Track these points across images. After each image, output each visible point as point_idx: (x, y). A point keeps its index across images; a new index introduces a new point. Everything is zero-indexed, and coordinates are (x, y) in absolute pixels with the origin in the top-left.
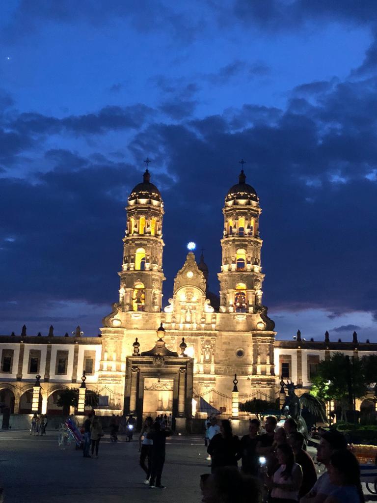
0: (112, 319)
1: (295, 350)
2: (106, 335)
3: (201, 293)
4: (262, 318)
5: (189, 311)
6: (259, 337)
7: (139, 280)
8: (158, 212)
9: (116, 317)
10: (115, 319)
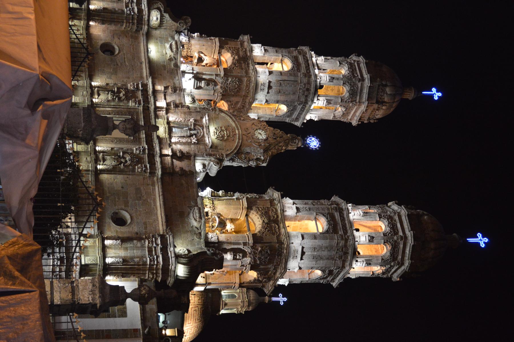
1: (138, 325)
5: (192, 132)
7: (236, 57)
8: (358, 101)
9: (167, 16)
10: (162, 16)
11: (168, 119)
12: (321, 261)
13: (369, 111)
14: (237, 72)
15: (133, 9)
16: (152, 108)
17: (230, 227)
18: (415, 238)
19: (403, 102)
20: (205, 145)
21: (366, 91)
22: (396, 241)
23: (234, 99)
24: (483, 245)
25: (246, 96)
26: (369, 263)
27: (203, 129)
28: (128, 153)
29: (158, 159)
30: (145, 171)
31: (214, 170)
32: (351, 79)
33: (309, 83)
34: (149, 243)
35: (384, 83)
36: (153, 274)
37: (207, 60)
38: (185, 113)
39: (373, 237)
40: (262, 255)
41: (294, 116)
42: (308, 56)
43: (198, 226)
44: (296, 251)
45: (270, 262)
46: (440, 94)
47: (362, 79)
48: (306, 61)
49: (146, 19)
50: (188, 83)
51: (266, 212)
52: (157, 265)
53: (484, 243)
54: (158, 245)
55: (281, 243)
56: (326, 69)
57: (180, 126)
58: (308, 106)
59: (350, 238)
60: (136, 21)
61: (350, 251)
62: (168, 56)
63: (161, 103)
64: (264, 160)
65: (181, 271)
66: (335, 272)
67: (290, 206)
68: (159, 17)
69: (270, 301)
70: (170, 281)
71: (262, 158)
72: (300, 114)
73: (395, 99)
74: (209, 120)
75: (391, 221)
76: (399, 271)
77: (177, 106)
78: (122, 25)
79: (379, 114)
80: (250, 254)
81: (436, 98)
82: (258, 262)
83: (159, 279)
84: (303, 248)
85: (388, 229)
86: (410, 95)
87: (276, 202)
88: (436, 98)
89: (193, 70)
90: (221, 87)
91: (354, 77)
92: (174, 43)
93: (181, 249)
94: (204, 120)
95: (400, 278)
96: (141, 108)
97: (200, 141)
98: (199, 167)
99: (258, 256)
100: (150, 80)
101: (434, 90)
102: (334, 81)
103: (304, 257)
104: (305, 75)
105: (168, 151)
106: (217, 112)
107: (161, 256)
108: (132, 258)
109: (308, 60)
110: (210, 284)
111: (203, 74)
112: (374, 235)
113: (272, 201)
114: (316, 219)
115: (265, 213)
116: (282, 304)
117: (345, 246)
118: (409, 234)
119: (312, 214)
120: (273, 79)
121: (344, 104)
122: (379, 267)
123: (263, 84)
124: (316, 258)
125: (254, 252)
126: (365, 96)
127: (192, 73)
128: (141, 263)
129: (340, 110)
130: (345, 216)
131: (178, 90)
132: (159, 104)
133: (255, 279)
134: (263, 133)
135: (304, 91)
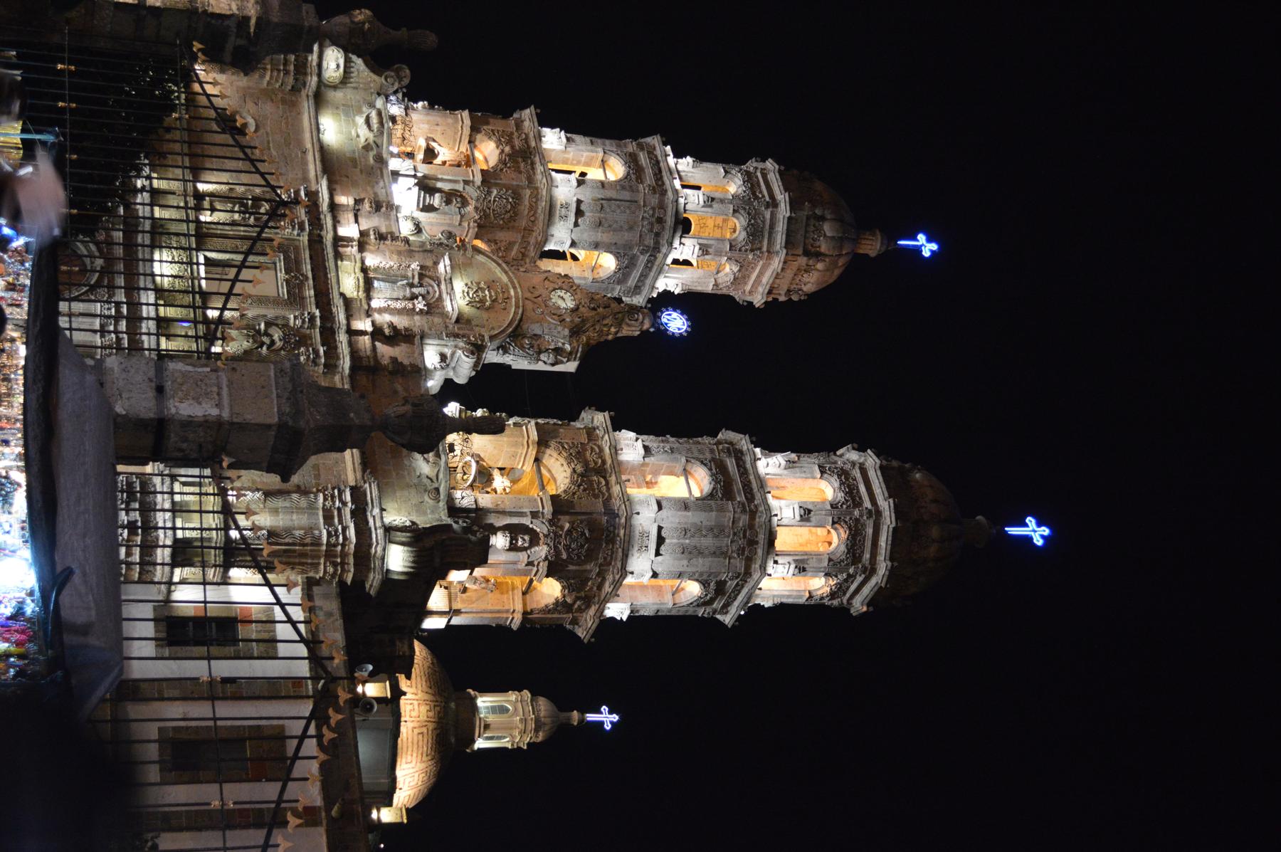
7: (507, 149)
8: (765, 249)
9: (358, 62)
10: (348, 61)
11: (363, 262)
12: (700, 560)
13: (789, 274)
14: (509, 177)
16: (328, 238)
17: (500, 482)
18: (899, 512)
19: (858, 261)
20: (444, 315)
21: (781, 227)
22: (857, 520)
23: (502, 236)
24: (1039, 542)
25: (528, 230)
26: (801, 569)
27: (439, 285)
28: (277, 325)
29: (342, 338)
30: (315, 363)
31: (463, 370)
32: (749, 202)
33: (662, 206)
34: (325, 499)
35: (818, 212)
36: (335, 565)
37: (445, 153)
38: (399, 253)
39: (810, 511)
40: (573, 540)
41: (631, 282)
42: (658, 152)
43: (433, 475)
44: (645, 535)
45: (591, 556)
46: (934, 247)
47: (774, 203)
48: (656, 163)
49: (314, 63)
50: (405, 195)
51: (578, 453)
52: (343, 545)
53: (1042, 537)
54: (344, 504)
55: (613, 515)
56: (697, 183)
57: (390, 278)
58: (660, 256)
59: (762, 508)
60: (292, 68)
61: (762, 538)
62: (362, 140)
63: (349, 229)
64: (570, 353)
65: (397, 559)
66: (731, 584)
67: (631, 447)
68: (342, 62)
69: (582, 721)
70: (373, 582)
71: (568, 347)
72: (643, 276)
73: (841, 248)
74: (452, 267)
75: (847, 479)
76: (866, 590)
77: (381, 237)
78: (262, 77)
79: (810, 283)
80: (546, 536)
81: (926, 253)
82: (564, 556)
83: (349, 578)
84: (660, 528)
86: (872, 246)
87: (600, 433)
88: (926, 253)
89: (415, 169)
90: (476, 208)
91: (756, 198)
92: (374, 114)
93: (396, 516)
94: (441, 267)
95: (868, 605)
96: (305, 238)
97: (434, 307)
98: (431, 357)
99: (563, 542)
100: (324, 183)
101: (922, 238)
102: (715, 205)
103: (662, 548)
104: (654, 191)
105: (363, 325)
106: (469, 253)
107: (352, 526)
108: (288, 531)
109: (658, 162)
110: (457, 612)
111: (438, 180)
112: (810, 507)
113: (591, 432)
114: (686, 473)
115: (577, 454)
116: (608, 727)
117: (751, 526)
118: (885, 505)
119: (676, 460)
120: (586, 195)
121: (736, 254)
122: (823, 579)
123: (566, 206)
124: (688, 552)
125: (555, 533)
126: (780, 238)
127: (415, 176)
128: (308, 540)
129: (729, 269)
130: (748, 466)
131: (383, 206)
132: (343, 231)
133: (557, 603)
134: (567, 296)
135: (652, 224)
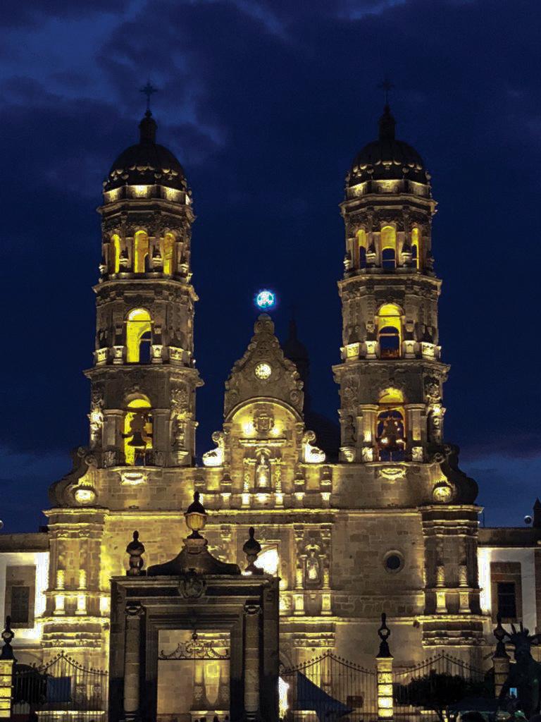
0: (75, 486)
2: (58, 528)
3: (293, 417)
4: (446, 474)
5: (263, 461)
6: (440, 521)
7: (136, 387)
8: (180, 217)
9: (82, 481)
10: (82, 488)
15: (81, 528)
27: (259, 447)
34: (440, 533)
85: (393, 223)
91: (153, 219)
104: (159, 293)
109: (131, 285)
